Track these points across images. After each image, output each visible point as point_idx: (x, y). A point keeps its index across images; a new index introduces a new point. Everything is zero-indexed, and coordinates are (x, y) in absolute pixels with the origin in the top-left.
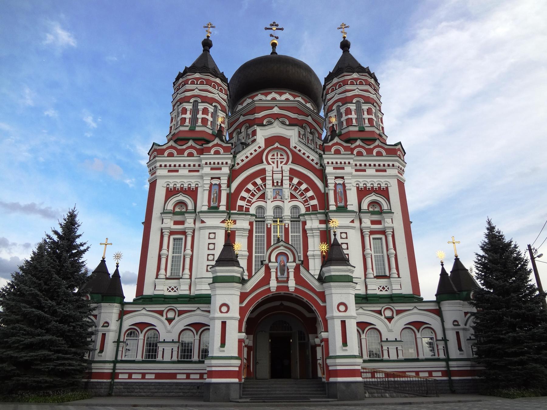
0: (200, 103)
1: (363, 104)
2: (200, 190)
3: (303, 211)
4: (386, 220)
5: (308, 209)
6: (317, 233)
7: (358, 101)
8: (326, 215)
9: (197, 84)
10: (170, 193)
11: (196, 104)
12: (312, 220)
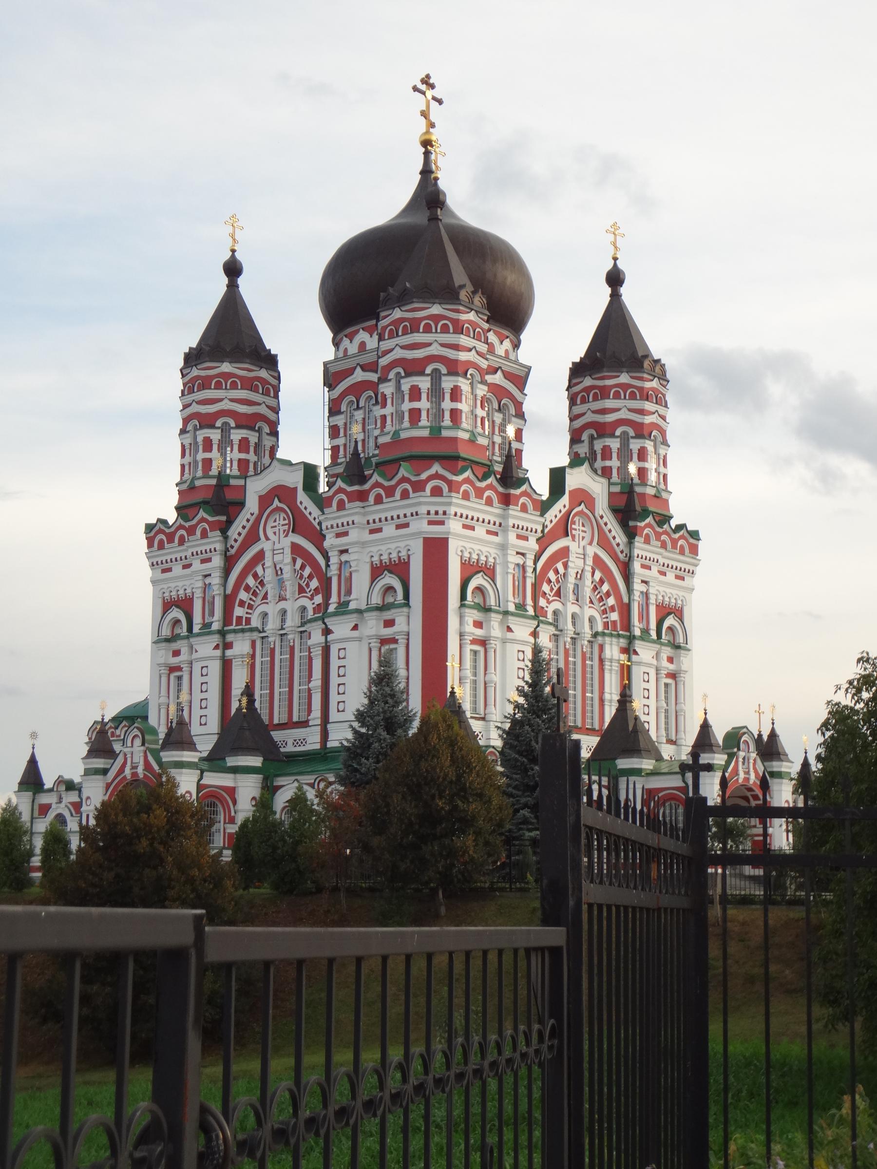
0: (444, 375)
1: (631, 441)
2: (498, 570)
3: (600, 628)
4: (682, 658)
5: (606, 625)
6: (616, 667)
7: (625, 433)
8: (631, 639)
9: (436, 332)
10: (470, 569)
11: (436, 376)
12: (611, 644)
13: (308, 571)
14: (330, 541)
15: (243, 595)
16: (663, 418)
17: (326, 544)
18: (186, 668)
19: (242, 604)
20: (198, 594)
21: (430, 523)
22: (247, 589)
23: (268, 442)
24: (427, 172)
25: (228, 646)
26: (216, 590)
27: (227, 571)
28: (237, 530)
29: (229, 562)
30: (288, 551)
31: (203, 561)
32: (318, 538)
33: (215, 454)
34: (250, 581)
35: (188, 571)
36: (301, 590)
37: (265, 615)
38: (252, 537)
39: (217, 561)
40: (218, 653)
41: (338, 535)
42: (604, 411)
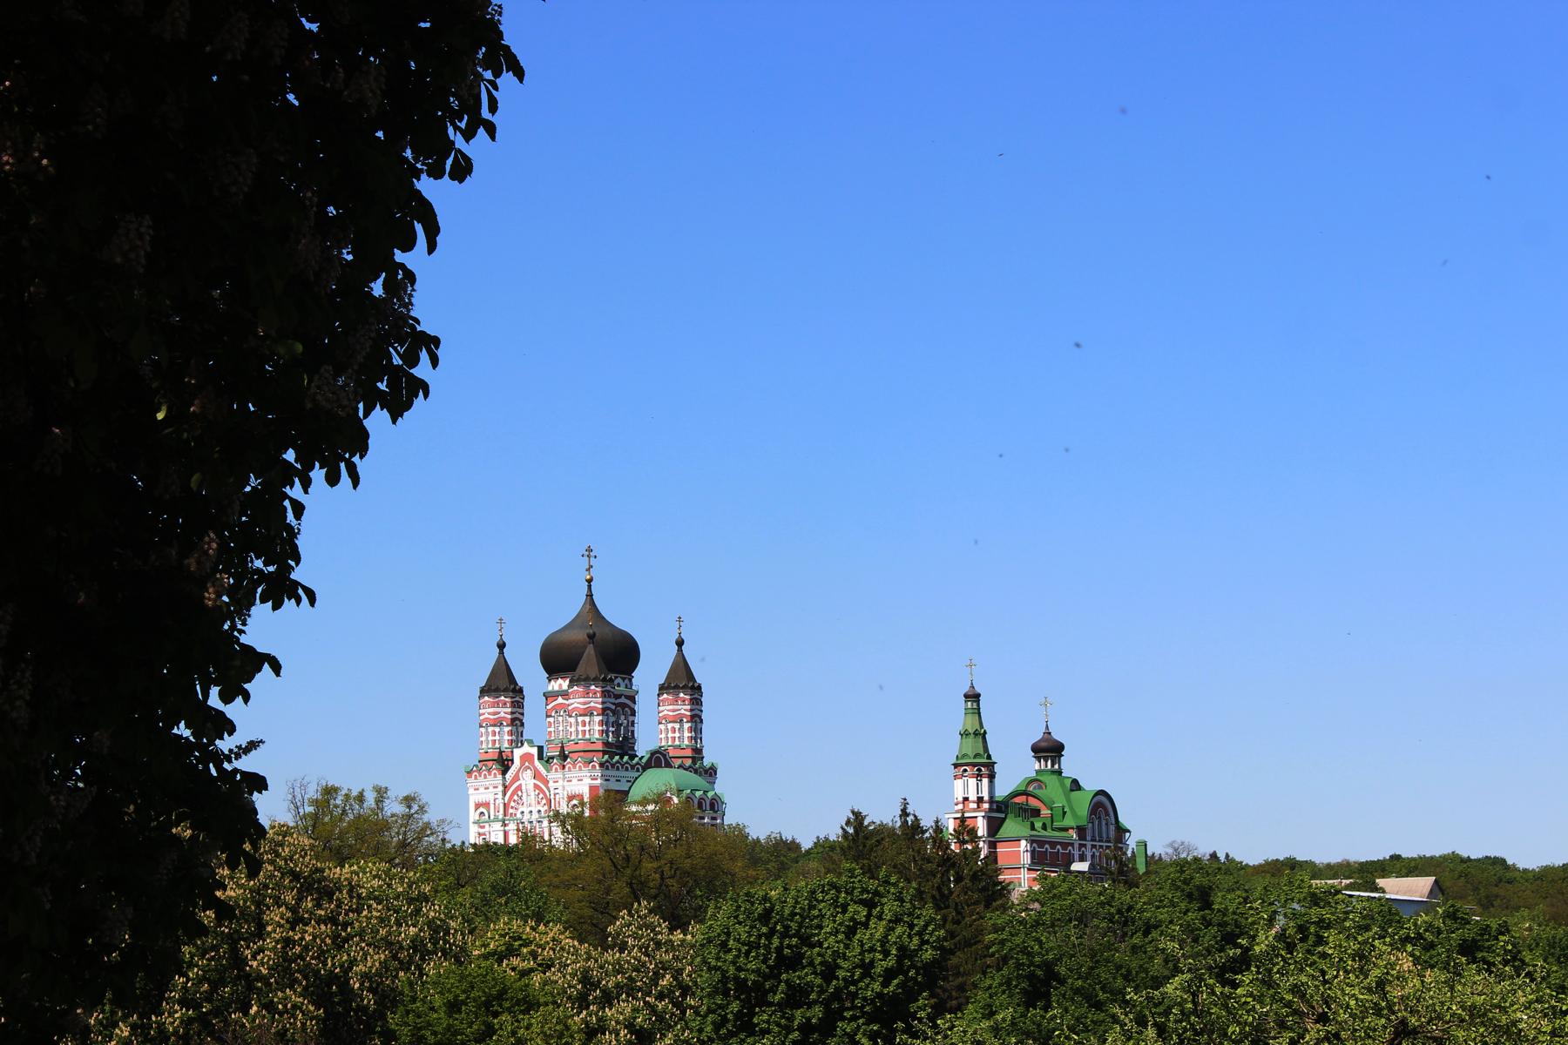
13: (541, 796)
14: (551, 784)
15: (512, 804)
16: (702, 711)
17: (549, 785)
18: (487, 833)
19: (512, 807)
20: (492, 802)
21: (592, 779)
22: (514, 801)
23: (520, 729)
24: (590, 596)
25: (505, 825)
26: (500, 802)
27: (504, 794)
28: (509, 775)
29: (506, 788)
30: (532, 785)
31: (494, 787)
32: (546, 782)
33: (497, 738)
34: (516, 798)
35: (487, 791)
36: (539, 803)
37: (523, 812)
38: (516, 778)
39: (501, 788)
40: (502, 828)
41: (555, 782)
42: (674, 711)
